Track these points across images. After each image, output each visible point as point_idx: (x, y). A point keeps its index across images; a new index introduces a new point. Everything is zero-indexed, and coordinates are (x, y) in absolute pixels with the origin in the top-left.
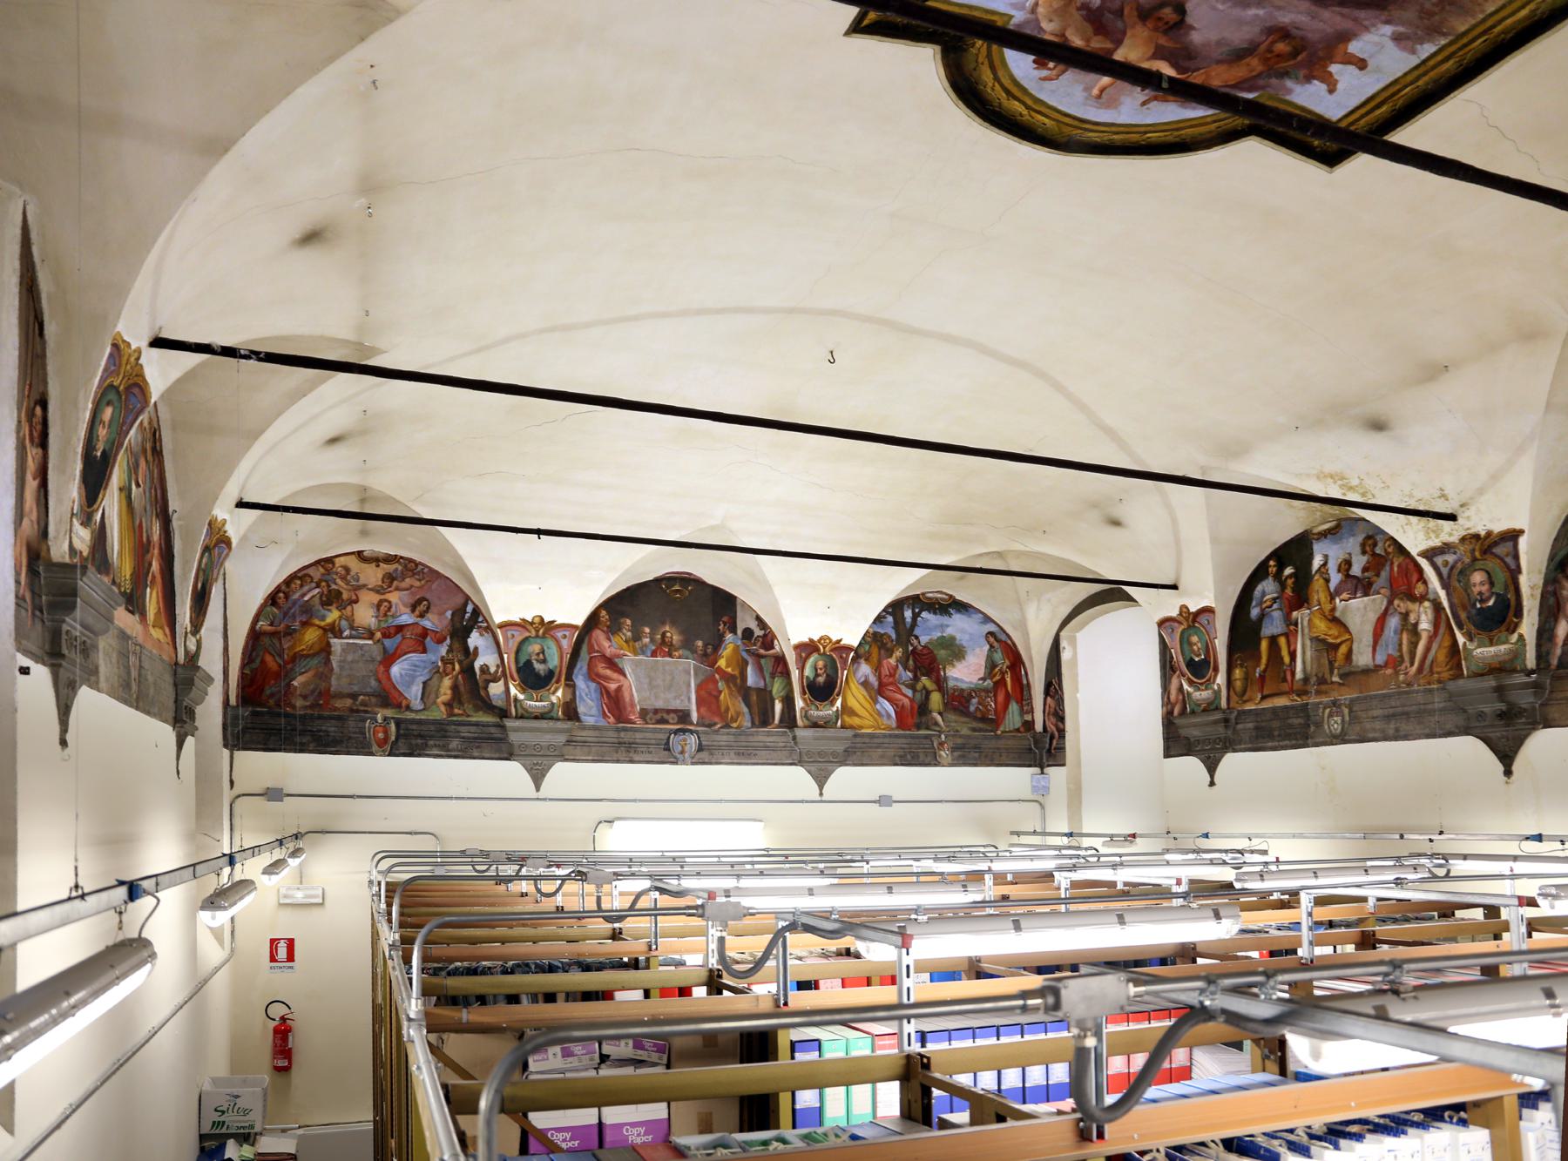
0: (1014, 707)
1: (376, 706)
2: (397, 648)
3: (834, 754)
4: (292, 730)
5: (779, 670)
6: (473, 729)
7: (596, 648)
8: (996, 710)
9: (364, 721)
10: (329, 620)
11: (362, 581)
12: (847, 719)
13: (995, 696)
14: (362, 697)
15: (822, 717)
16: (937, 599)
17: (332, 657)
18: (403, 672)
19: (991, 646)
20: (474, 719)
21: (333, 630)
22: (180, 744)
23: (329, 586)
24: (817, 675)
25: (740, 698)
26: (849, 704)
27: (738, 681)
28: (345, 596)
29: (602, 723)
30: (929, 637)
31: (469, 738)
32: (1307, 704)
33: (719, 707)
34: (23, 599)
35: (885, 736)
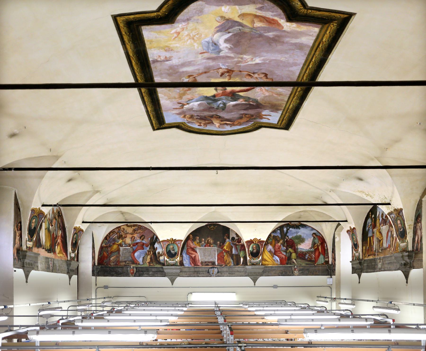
0: (321, 257)
1: (131, 264)
2: (136, 249)
3: (259, 273)
4: (111, 271)
5: (242, 249)
6: (155, 269)
7: (189, 245)
8: (315, 258)
9: (128, 268)
10: (119, 242)
11: (128, 232)
12: (263, 262)
13: (315, 253)
14: (127, 262)
15: (255, 262)
16: (295, 224)
17: (120, 252)
18: (138, 255)
19: (314, 238)
20: (156, 266)
21: (121, 245)
22: (70, 278)
23: (119, 234)
24: (253, 250)
25: (230, 258)
26: (265, 258)
27: (230, 252)
28: (123, 236)
29: (190, 266)
30: (292, 236)
31: (154, 271)
32: (375, 258)
33: (224, 260)
34: (16, 258)
35: (276, 267)
